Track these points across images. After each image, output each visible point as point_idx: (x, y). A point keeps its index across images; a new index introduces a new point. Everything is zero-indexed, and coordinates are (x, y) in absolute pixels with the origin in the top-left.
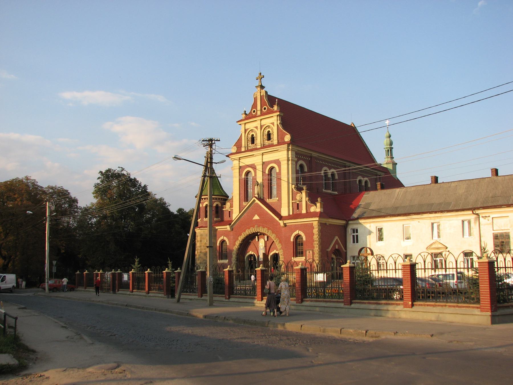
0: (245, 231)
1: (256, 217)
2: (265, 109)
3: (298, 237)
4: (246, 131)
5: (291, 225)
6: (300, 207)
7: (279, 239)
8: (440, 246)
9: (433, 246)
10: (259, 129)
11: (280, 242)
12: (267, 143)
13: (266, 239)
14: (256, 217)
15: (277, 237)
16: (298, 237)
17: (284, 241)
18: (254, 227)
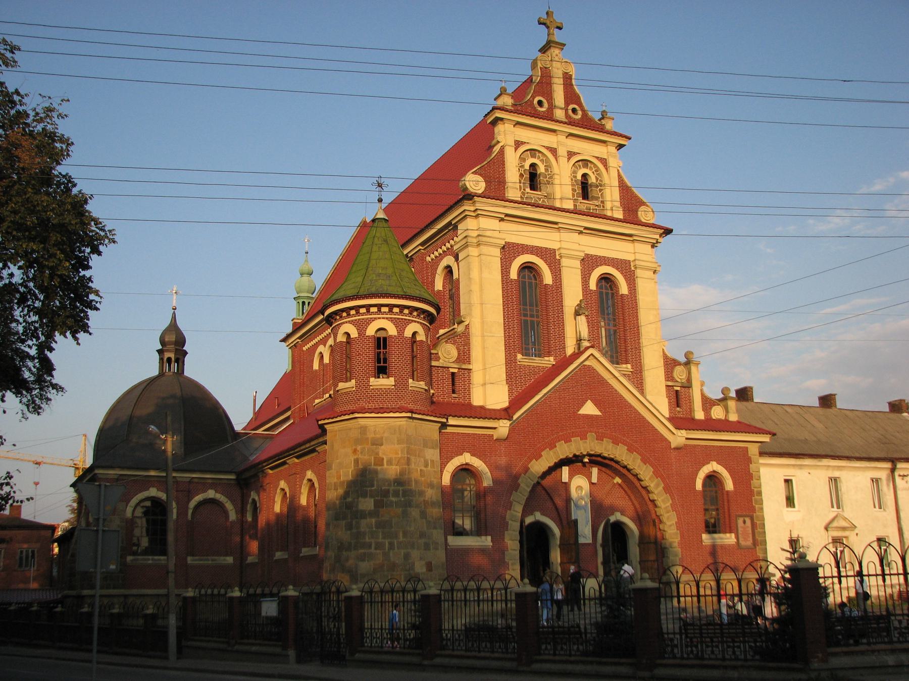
0: (552, 446)
1: (589, 409)
2: (574, 111)
3: (713, 478)
4: (518, 144)
5: (695, 446)
6: (683, 402)
7: (663, 480)
8: (844, 524)
9: (835, 524)
10: (563, 160)
11: (667, 489)
12: (583, 205)
13: (594, 479)
14: (589, 409)
15: (657, 474)
16: (713, 478)
17: (678, 487)
18: (584, 437)
